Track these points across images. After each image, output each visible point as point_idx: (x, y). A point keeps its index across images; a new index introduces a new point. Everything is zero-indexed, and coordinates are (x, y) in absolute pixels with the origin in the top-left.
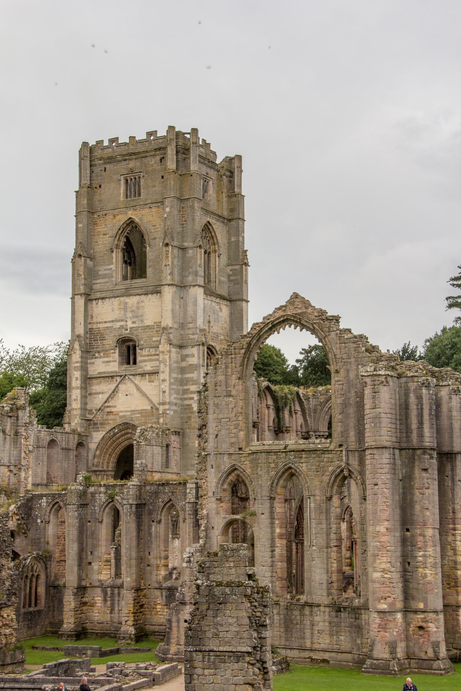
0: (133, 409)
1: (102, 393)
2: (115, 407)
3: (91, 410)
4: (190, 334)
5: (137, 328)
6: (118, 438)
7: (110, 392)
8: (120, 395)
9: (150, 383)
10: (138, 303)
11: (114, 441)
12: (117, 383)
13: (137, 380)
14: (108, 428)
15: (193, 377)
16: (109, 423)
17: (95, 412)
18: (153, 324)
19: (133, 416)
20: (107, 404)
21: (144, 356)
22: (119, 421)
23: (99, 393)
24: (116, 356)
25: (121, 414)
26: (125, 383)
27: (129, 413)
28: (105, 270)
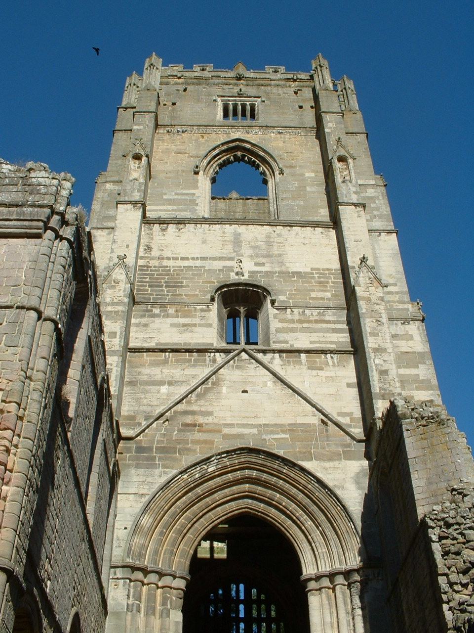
0: (262, 421)
1: (170, 383)
2: (209, 414)
3: (132, 418)
4: (394, 302)
5: (268, 274)
6: (211, 492)
7: (194, 383)
8: (224, 390)
9: (314, 372)
10: (268, 237)
11: (200, 499)
12: (216, 366)
13: (276, 362)
14: (186, 461)
15: (418, 375)
16: (188, 450)
17: (144, 424)
18: (309, 270)
19: (264, 437)
20: (179, 407)
21: (292, 321)
22: (222, 445)
23: (161, 383)
24: (214, 313)
25: (226, 431)
26: (238, 367)
27: (255, 431)
28: (176, 194)
